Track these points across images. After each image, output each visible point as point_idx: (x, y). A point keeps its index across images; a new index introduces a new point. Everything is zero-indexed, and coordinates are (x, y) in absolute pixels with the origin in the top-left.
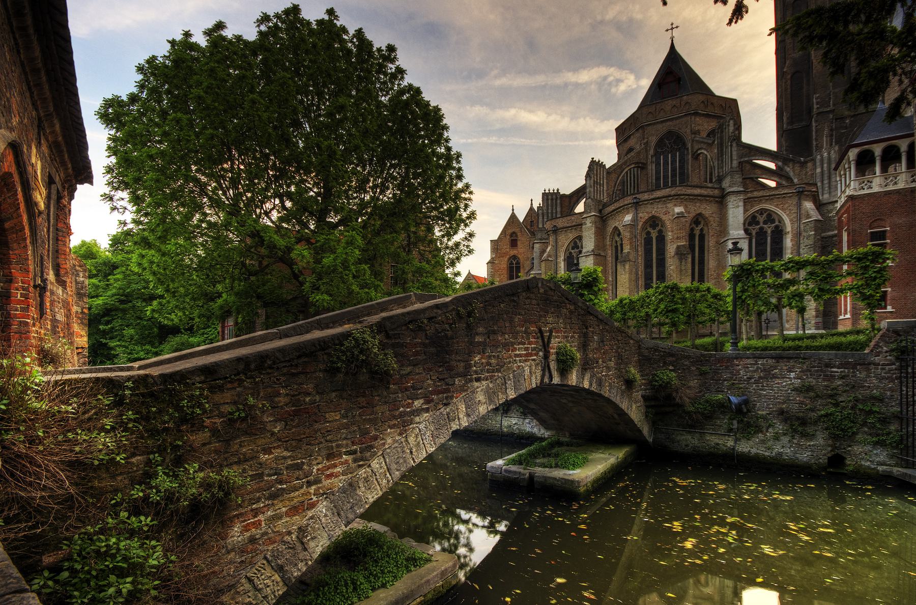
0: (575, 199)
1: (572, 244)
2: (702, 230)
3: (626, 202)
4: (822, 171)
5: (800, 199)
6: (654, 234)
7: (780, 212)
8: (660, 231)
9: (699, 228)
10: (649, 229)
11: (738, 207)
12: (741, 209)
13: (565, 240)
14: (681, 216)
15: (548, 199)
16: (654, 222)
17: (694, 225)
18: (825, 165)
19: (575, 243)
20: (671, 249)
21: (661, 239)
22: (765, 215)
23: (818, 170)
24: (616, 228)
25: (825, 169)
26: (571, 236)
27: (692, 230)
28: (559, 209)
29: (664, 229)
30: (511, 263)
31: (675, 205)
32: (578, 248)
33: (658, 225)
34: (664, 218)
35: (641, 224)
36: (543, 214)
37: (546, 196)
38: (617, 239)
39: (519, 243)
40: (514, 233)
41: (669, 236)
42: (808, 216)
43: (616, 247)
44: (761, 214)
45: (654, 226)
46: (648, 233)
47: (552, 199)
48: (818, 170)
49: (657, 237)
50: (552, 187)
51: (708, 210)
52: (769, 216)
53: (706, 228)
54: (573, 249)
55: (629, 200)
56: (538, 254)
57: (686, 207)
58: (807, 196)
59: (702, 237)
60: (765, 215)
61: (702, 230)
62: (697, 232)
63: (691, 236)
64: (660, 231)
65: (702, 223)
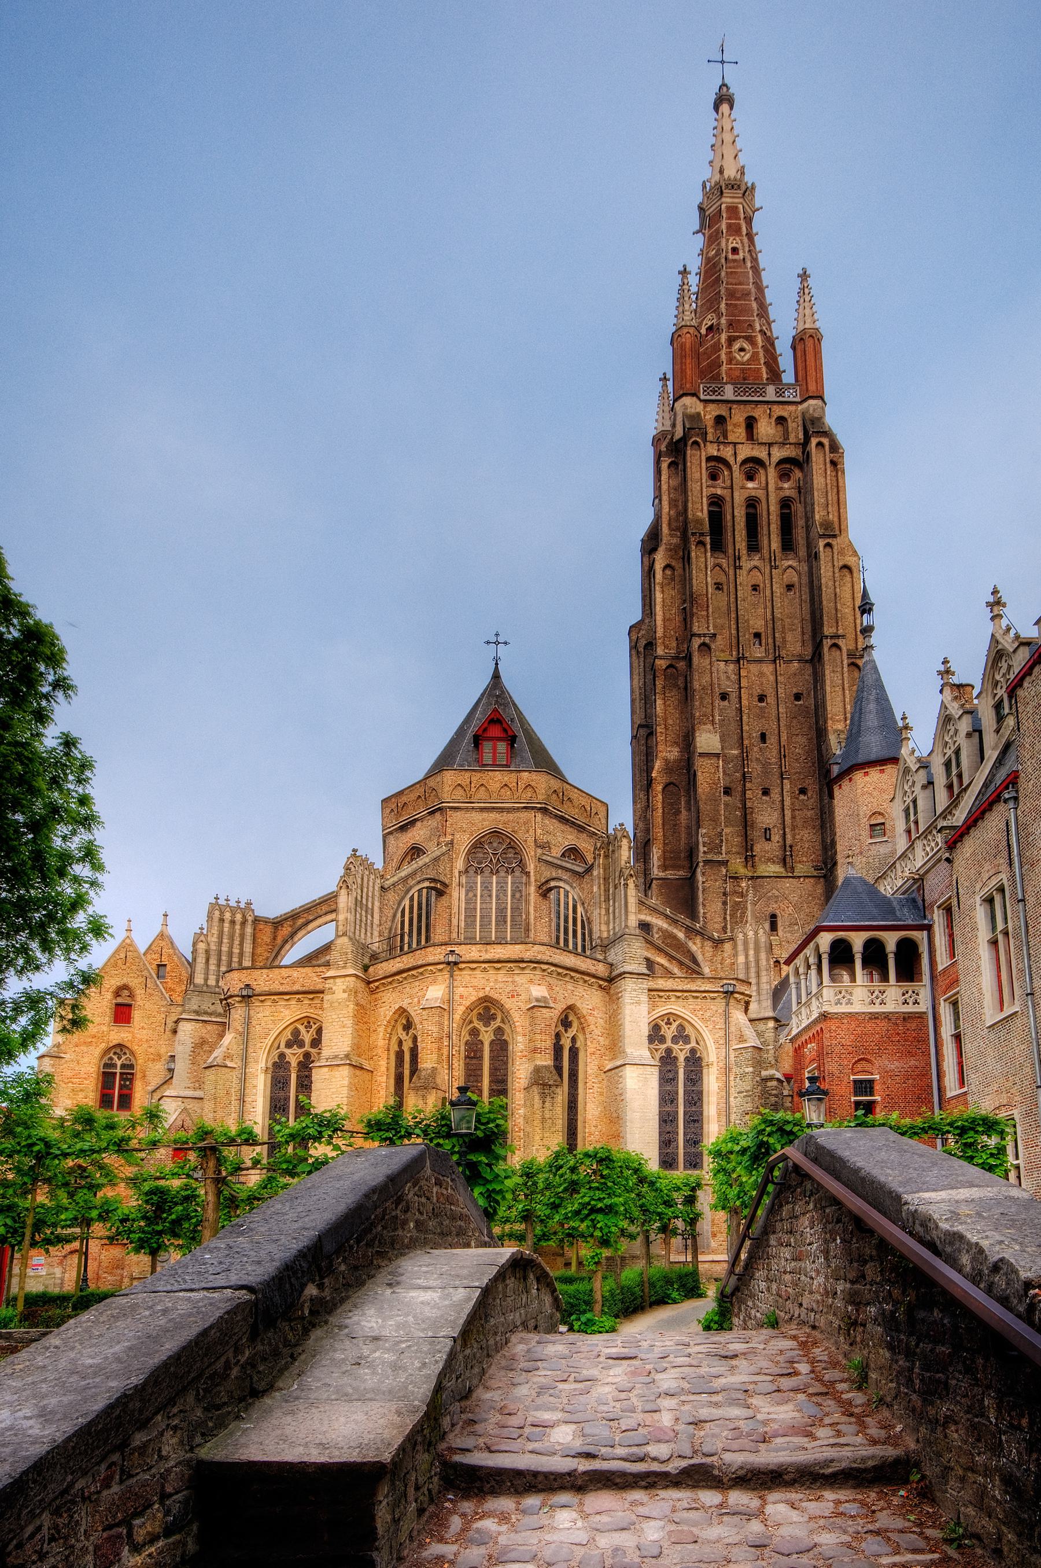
0: (286, 930)
1: (288, 1035)
2: (574, 1039)
3: (431, 959)
4: (747, 963)
5: (727, 1005)
6: (487, 1036)
7: (699, 1024)
8: (499, 1031)
9: (571, 1033)
10: (478, 1024)
11: (638, 1003)
12: (644, 1008)
13: (273, 1021)
14: (541, 1004)
15: (222, 920)
16: (487, 1009)
17: (561, 1029)
18: (751, 952)
19: (296, 1033)
20: (521, 1072)
21: (501, 1047)
22: (674, 1025)
23: (741, 959)
24: (402, 1011)
25: (751, 958)
26: (289, 1013)
27: (558, 1036)
28: (248, 948)
29: (505, 1027)
30: (110, 1065)
31: (531, 981)
32: (301, 1044)
33: (493, 1017)
34: (509, 1004)
35: (460, 1011)
36: (207, 952)
37: (218, 910)
38: (403, 1035)
39: (136, 1015)
40: (125, 987)
41: (519, 1044)
42: (742, 1039)
43: (400, 1055)
44: (669, 1023)
45: (487, 1017)
46: (474, 1032)
47: (233, 922)
48: (741, 959)
49: (492, 1043)
50: (237, 893)
51: (589, 1001)
52: (681, 1028)
53: (580, 1036)
54: (289, 1045)
55: (436, 954)
56: (188, 1048)
57: (550, 987)
58: (738, 1001)
59: (574, 1053)
60: (674, 1025)
61: (574, 1039)
62: (566, 1043)
63: (558, 1049)
64: (499, 1031)
65: (575, 1024)
